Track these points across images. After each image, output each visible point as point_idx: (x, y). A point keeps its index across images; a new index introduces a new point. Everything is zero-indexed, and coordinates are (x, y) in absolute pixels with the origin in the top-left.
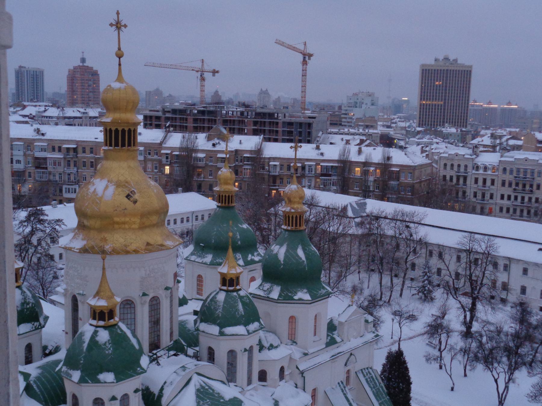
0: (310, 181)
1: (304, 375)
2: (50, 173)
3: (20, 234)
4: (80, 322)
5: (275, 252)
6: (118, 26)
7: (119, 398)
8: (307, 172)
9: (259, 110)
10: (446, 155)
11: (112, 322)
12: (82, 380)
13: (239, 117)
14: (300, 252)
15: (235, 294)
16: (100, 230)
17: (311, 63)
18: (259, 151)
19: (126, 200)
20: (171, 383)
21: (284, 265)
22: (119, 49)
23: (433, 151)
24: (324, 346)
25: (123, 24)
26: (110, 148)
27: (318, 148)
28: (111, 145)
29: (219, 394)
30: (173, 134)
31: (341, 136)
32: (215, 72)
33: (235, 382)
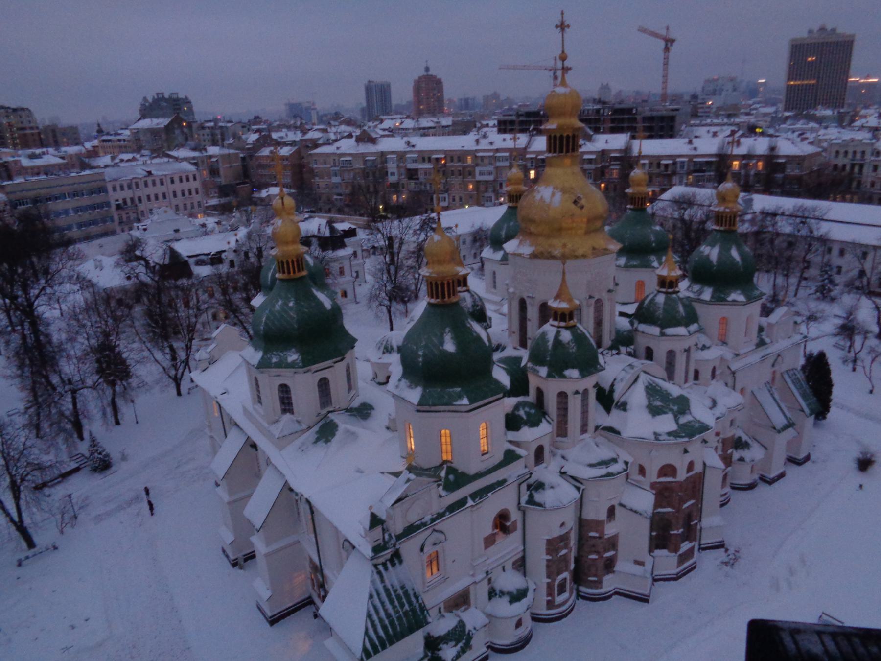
0: (681, 178)
2: (421, 183)
3: (415, 242)
4: (529, 323)
5: (706, 252)
8: (678, 169)
9: (618, 106)
10: (839, 141)
11: (572, 323)
12: (550, 375)
14: (734, 253)
15: (675, 296)
16: (548, 237)
17: (674, 49)
18: (627, 149)
19: (573, 206)
20: (622, 380)
22: (563, 52)
23: (820, 137)
24: (754, 347)
26: (554, 155)
27: (690, 142)
28: (555, 152)
29: (666, 391)
30: (536, 137)
31: (708, 128)
33: (673, 380)
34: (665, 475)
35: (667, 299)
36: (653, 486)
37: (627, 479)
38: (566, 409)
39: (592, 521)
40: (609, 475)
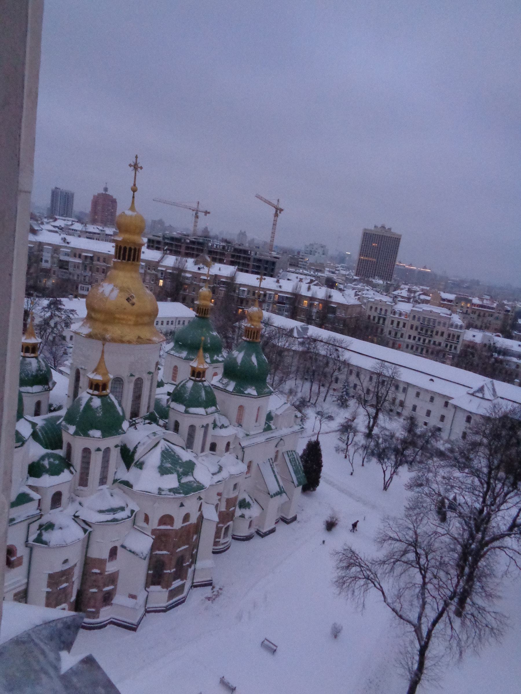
0: (268, 306)
1: (244, 450)
2: (70, 274)
3: (41, 317)
4: (80, 389)
5: (235, 356)
6: (136, 167)
7: (103, 450)
8: (267, 299)
9: (237, 247)
10: (373, 300)
11: (104, 392)
12: (76, 433)
13: (221, 250)
14: (254, 359)
15: (200, 383)
16: (104, 322)
17: (281, 216)
18: (233, 278)
19: (126, 302)
20: (144, 444)
21: (241, 367)
22: (135, 185)
23: (364, 296)
24: (262, 431)
25: (139, 166)
27: (278, 281)
28: (119, 259)
29: (178, 456)
30: (169, 255)
31: (297, 275)
32: (206, 213)
33: (192, 449)
34: (165, 524)
35: (194, 386)
36: (154, 532)
37: (134, 524)
38: (88, 463)
39: (95, 560)
40: (115, 520)
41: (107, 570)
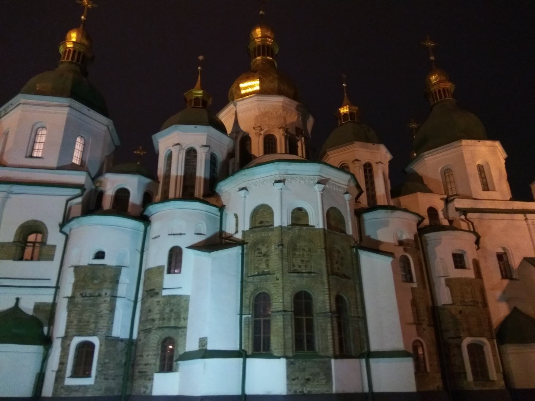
41: (165, 286)
